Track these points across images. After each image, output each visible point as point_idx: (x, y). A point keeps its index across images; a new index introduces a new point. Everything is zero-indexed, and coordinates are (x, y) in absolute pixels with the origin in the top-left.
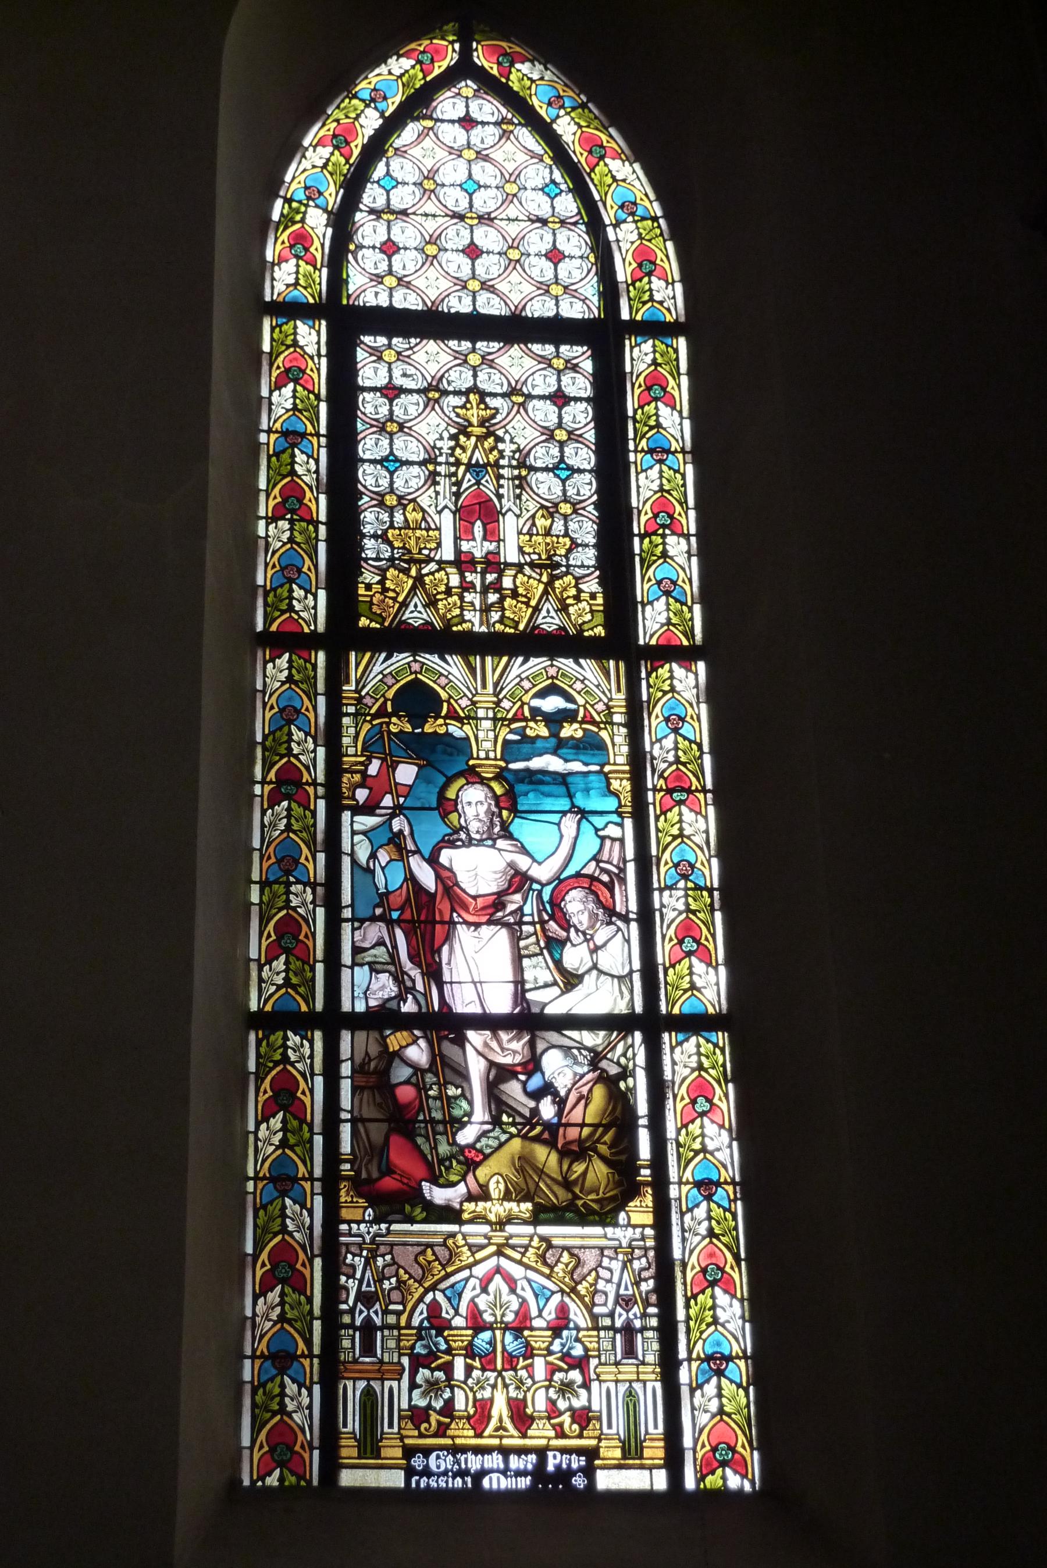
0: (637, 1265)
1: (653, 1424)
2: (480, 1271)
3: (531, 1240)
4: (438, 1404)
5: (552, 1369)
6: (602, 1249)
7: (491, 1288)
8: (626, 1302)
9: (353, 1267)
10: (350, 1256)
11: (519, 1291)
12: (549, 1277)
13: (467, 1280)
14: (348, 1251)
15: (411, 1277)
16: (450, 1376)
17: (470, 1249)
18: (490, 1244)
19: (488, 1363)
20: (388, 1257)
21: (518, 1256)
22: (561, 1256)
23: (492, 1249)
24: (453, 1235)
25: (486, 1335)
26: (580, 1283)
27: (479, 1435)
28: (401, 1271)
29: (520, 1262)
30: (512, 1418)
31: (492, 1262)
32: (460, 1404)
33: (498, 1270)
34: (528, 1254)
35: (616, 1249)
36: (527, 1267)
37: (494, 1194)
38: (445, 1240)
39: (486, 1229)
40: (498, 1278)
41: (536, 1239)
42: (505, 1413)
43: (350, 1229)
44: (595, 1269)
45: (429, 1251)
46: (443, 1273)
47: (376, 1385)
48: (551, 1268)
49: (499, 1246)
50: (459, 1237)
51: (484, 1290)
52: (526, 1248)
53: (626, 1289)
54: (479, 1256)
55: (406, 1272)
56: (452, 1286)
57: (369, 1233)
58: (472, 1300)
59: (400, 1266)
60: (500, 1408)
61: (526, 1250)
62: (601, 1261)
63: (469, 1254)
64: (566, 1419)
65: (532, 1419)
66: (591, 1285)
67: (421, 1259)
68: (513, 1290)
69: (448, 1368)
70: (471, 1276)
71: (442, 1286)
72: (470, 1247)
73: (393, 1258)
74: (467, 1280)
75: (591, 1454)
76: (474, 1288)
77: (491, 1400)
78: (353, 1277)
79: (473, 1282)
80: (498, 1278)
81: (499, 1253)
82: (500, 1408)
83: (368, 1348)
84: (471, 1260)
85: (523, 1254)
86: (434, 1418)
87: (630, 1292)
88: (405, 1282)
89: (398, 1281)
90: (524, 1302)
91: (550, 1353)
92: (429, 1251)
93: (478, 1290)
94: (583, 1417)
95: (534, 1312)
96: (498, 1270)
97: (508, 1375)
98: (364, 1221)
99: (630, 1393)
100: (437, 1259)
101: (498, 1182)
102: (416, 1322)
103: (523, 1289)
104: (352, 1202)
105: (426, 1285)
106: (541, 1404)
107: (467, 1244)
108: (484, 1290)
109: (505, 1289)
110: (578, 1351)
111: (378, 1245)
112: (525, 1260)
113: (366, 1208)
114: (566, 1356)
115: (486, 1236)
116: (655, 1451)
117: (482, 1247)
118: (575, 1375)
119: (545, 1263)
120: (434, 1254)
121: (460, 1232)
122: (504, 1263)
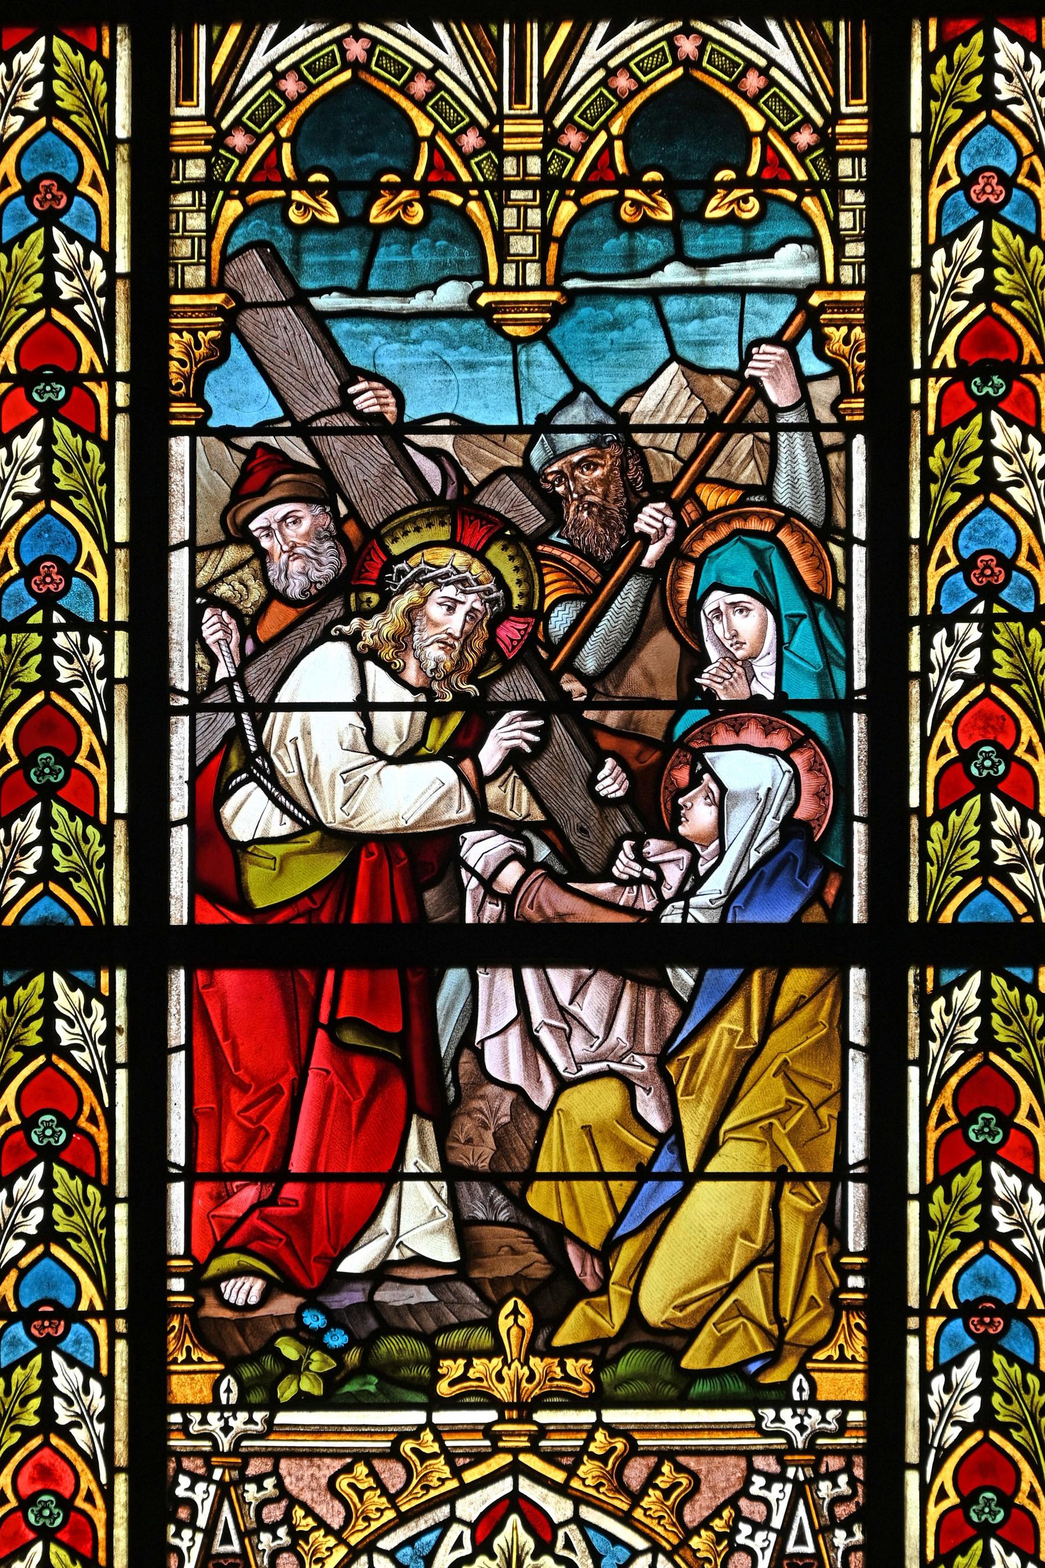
2: (470, 1507)
3: (590, 1438)
6: (748, 1454)
7: (500, 1542)
9: (191, 1504)
10: (184, 1481)
11: (559, 1550)
12: (626, 1519)
13: (444, 1526)
14: (180, 1470)
15: (321, 1523)
17: (450, 1461)
18: (496, 1450)
20: (269, 1483)
21: (559, 1476)
22: (656, 1472)
23: (505, 1459)
24: (415, 1433)
26: (696, 1531)
28: (299, 1512)
29: (561, 1490)
31: (505, 1486)
33: (514, 1502)
34: (581, 1471)
35: (779, 1455)
36: (579, 1500)
37: (512, 1345)
38: (396, 1443)
39: (491, 1416)
40: (514, 1519)
41: (600, 1435)
43: (187, 1422)
44: (732, 1502)
45: (361, 1469)
46: (390, 1515)
48: (636, 1499)
49: (515, 1451)
50: (428, 1436)
52: (579, 1455)
53: (801, 1540)
54: (470, 1476)
55: (309, 1512)
56: (410, 1542)
57: (226, 1429)
59: (294, 1502)
61: (579, 1462)
62: (748, 1482)
63: (446, 1472)
66: (719, 1537)
67: (343, 1483)
68: (544, 1547)
70: (453, 1519)
71: (387, 1543)
72: (450, 1457)
73: (280, 1485)
74: (444, 1526)
76: (458, 1544)
78: (192, 1524)
79: (455, 1530)
80: (514, 1519)
81: (516, 1469)
84: (454, 1484)
85: (571, 1472)
87: (810, 1549)
88: (305, 1536)
89: (292, 1532)
92: (361, 1469)
93: (467, 1549)
96: (514, 1502)
98: (216, 1405)
100: (380, 1485)
101: (515, 1312)
103: (568, 1545)
104: (188, 1360)
105: (353, 1540)
107: (443, 1448)
111: (247, 1457)
112: (575, 1484)
113: (223, 1374)
115: (486, 1430)
117: (479, 1457)
119: (622, 1488)
120: (373, 1473)
121: (429, 1424)
122: (526, 1487)
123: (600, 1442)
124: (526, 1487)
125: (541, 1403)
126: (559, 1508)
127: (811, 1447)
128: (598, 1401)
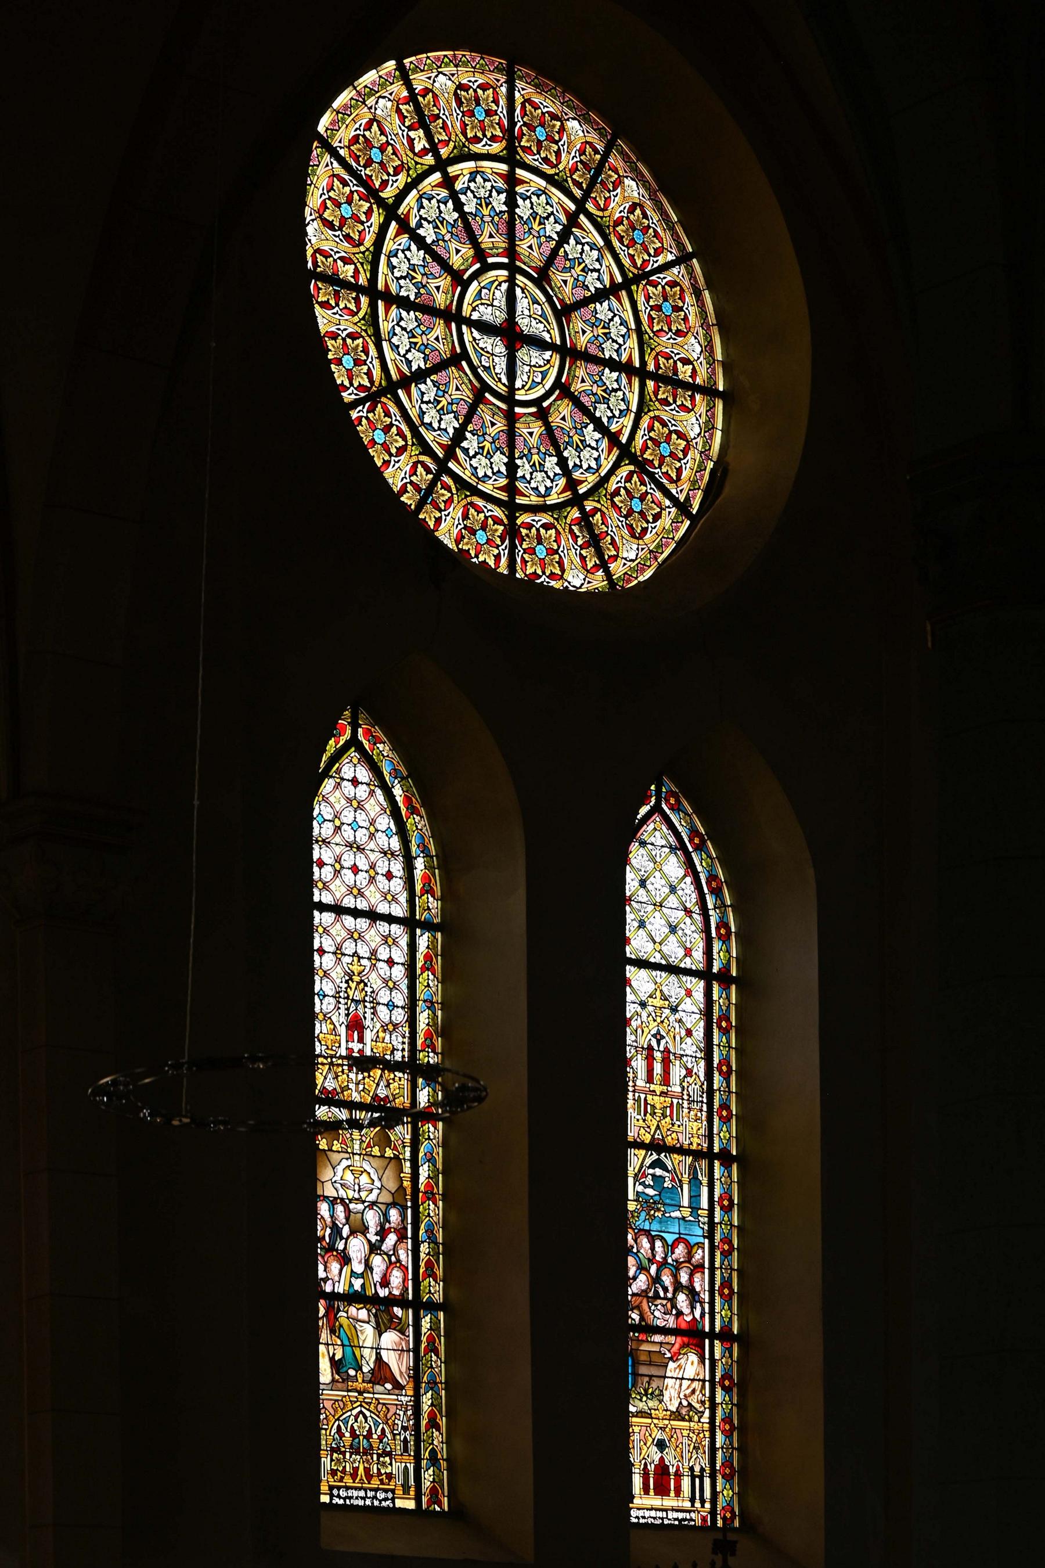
2: (355, 1412)
5: (379, 1456)
16: (344, 1457)
31: (359, 1409)
32: (348, 1469)
33: (361, 1412)
51: (356, 1421)
58: (352, 1426)
60: (361, 1471)
68: (366, 1422)
69: (344, 1453)
75: (393, 1491)
81: (361, 1406)
82: (361, 1471)
94: (389, 1476)
96: (361, 1412)
106: (375, 1471)
108: (356, 1421)
110: (388, 1449)
118: (387, 1459)
126: (368, 1414)
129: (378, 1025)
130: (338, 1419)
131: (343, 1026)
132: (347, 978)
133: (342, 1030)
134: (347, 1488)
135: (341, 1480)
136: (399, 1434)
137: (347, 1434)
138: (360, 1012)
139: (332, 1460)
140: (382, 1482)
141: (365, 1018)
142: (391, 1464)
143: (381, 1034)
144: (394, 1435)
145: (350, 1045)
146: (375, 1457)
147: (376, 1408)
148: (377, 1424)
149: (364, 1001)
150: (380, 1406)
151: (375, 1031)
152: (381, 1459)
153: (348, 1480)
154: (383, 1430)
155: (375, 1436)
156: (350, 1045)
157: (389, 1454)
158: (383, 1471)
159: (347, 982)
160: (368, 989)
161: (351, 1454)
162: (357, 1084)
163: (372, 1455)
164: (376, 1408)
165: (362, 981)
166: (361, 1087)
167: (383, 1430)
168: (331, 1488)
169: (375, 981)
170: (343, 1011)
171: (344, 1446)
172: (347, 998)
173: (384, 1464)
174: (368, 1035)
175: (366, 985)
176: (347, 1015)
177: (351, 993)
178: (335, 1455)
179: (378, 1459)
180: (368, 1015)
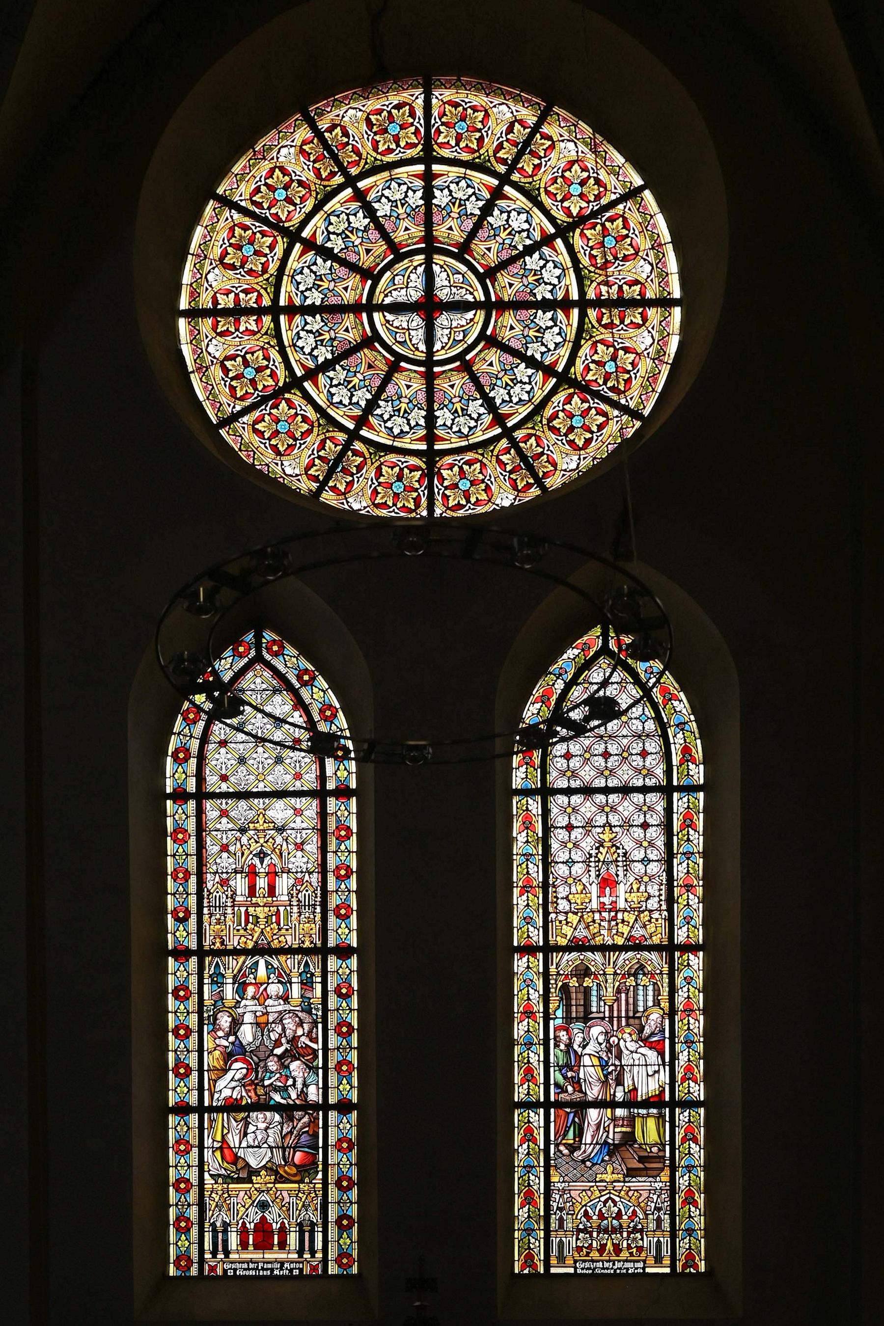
0: (663, 1196)
1: (666, 1252)
2: (603, 1199)
4: (586, 1245)
5: (629, 1233)
8: (659, 1209)
16: (591, 1236)
19: (606, 1231)
25: (605, 1222)
27: (601, 1256)
30: (614, 1250)
31: (608, 1196)
32: (594, 1244)
33: (610, 1198)
36: (621, 1198)
42: (612, 1249)
47: (564, 1239)
51: (605, 1206)
58: (600, 1210)
60: (609, 1246)
64: (634, 1250)
65: (621, 1250)
68: (615, 1205)
69: (591, 1234)
72: (599, 1191)
75: (644, 1262)
77: (606, 1244)
81: (610, 1193)
82: (609, 1246)
83: (561, 1226)
86: (584, 1250)
90: (620, 1210)
91: (629, 1227)
94: (640, 1249)
95: (624, 1213)
96: (610, 1198)
97: (613, 1236)
99: (659, 1242)
102: (579, 1217)
106: (625, 1245)
108: (605, 1206)
109: (612, 1205)
110: (640, 1226)
114: (635, 1227)
116: (667, 1261)
118: (638, 1235)
123: (624, 1188)
124: (612, 1196)
125: (615, 1181)
126: (617, 1199)
127: (660, 1189)
128: (624, 1182)
129: (632, 879)
130: (585, 1205)
131: (594, 885)
132: (597, 845)
133: (594, 889)
134: (593, 1261)
135: (588, 1254)
136: (653, 1214)
137: (595, 1217)
138: (613, 871)
139: (577, 1239)
140: (631, 1254)
141: (617, 875)
142: (642, 1239)
143: (635, 887)
144: (647, 1215)
145: (602, 900)
146: (625, 1234)
147: (627, 1194)
148: (627, 1208)
149: (617, 861)
150: (631, 1193)
151: (629, 884)
152: (632, 1236)
153: (595, 1255)
154: (634, 1212)
155: (625, 1217)
156: (602, 900)
157: (641, 1231)
158: (633, 1246)
159: (597, 848)
160: (620, 851)
161: (599, 1233)
162: (610, 929)
163: (621, 1233)
164: (627, 1194)
165: (614, 845)
166: (614, 932)
167: (634, 1212)
168: (575, 1262)
169: (628, 844)
170: (593, 874)
171: (591, 1227)
172: (599, 861)
173: (635, 1239)
174: (621, 889)
175: (618, 848)
176: (598, 876)
177: (601, 858)
178: (581, 1235)
179: (629, 1236)
180: (621, 873)
